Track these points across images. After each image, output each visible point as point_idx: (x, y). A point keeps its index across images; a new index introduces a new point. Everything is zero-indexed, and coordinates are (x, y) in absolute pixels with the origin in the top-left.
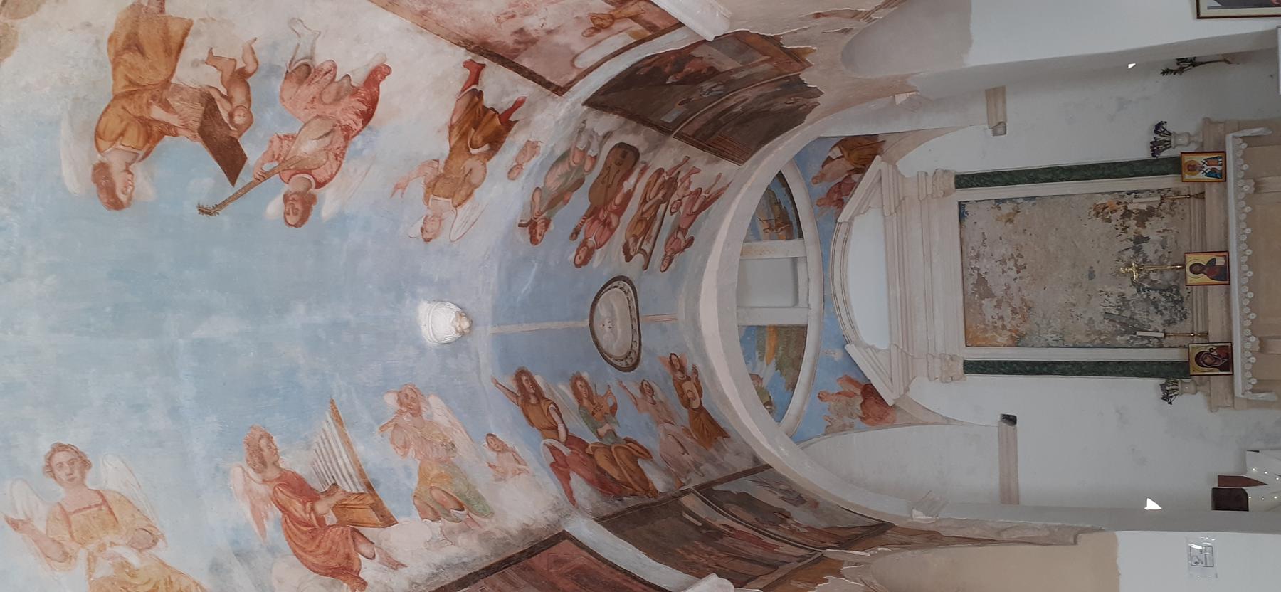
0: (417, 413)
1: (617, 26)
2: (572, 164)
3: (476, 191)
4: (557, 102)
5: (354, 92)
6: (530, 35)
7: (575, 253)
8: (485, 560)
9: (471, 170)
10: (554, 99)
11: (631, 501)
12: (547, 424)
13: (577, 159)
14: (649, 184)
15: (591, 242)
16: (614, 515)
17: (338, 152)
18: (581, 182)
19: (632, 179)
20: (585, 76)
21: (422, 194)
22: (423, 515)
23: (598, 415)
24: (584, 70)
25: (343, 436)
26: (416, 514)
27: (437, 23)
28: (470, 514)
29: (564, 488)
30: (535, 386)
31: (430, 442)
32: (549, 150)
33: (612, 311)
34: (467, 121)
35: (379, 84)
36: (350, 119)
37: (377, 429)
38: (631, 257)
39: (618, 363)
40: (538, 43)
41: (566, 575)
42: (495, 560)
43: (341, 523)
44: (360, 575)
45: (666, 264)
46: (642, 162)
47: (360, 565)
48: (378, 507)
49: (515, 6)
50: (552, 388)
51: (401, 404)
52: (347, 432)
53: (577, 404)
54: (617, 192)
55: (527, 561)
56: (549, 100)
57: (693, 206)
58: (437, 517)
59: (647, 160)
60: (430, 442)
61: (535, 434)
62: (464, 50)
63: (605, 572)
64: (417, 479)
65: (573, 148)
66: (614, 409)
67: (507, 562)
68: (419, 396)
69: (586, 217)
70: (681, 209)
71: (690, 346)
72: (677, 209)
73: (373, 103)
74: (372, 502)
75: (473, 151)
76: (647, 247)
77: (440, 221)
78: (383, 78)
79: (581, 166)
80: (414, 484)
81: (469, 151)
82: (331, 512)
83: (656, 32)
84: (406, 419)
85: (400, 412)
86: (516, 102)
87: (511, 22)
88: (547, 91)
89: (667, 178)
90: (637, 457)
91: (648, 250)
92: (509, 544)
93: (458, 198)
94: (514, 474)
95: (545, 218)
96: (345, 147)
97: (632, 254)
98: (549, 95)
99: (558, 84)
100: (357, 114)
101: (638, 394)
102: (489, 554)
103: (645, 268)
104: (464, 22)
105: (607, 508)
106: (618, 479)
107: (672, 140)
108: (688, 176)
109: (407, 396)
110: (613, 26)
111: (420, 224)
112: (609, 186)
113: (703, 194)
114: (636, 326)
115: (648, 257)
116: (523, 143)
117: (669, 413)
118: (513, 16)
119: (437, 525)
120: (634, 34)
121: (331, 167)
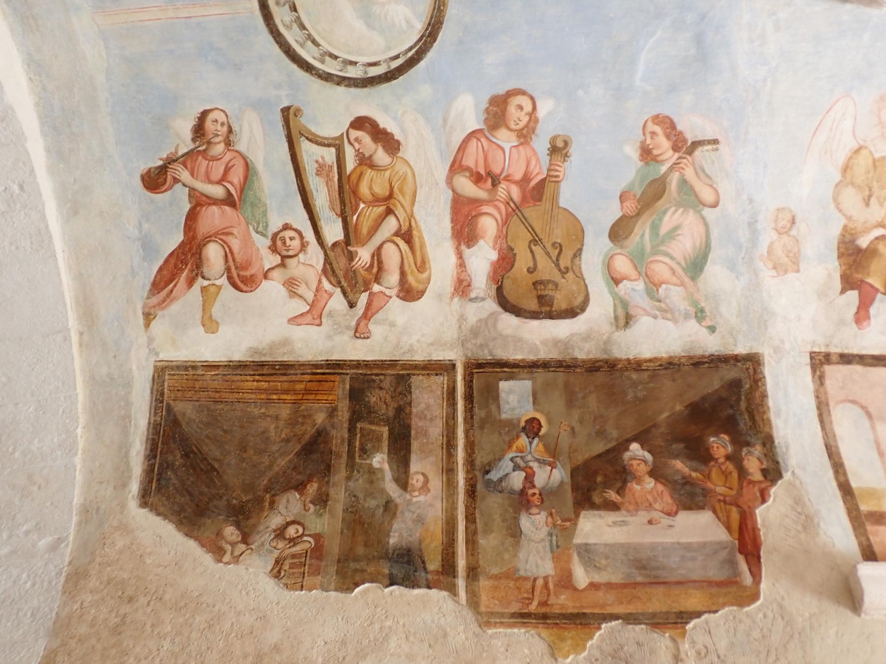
3: (838, 177)
9: (867, 204)
15: (506, 139)
79: (639, 260)
88: (839, 350)
93: (863, 162)
112: (536, 240)
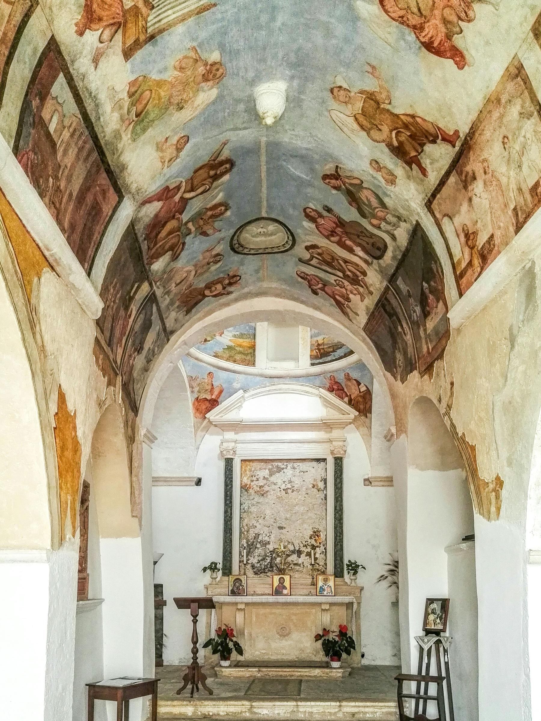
0: (205, 78)
1: (467, 250)
2: (377, 210)
4: (421, 202)
5: (449, 37)
6: (470, 185)
7: (314, 208)
8: (102, 135)
10: (424, 199)
11: (144, 247)
12: (195, 183)
13: (380, 214)
14: (357, 265)
15: (321, 221)
16: (136, 234)
17: (405, 19)
18: (363, 215)
19: (361, 253)
20: (437, 224)
21: (367, 89)
22: (132, 84)
23: (201, 222)
24: (441, 223)
25: (189, 15)
26: (132, 78)
27: (490, 112)
28: (134, 123)
29: (154, 196)
30: (223, 174)
31: (184, 89)
32: (388, 193)
33: (271, 235)
34: (416, 129)
35: (452, 58)
36: (429, 31)
37: (195, 44)
38: (308, 251)
39: (236, 237)
40: (463, 191)
41: (95, 199)
42: (102, 142)
43: (125, 12)
44: (87, 30)
45: (302, 275)
46: (372, 262)
47: (95, 30)
48: (137, 45)
49: (492, 175)
51: (211, 65)
52: (192, 18)
53: (208, 206)
54: (354, 242)
55: (102, 169)
56: (423, 196)
57: (339, 295)
58: (131, 95)
59: (373, 265)
60: (184, 89)
61: (188, 174)
62: (468, 132)
63: (99, 228)
64: (157, 79)
65: (386, 211)
66: (205, 234)
67: (102, 154)
68: (218, 80)
69: (339, 218)
70: (338, 288)
71: (246, 290)
72: (338, 285)
73: (438, 52)
74: (141, 41)
75: (394, 133)
76: (314, 262)
77: (345, 102)
78: (456, 63)
79: (375, 216)
80: (155, 76)
81: (394, 130)
82: (133, 4)
83: (459, 278)
84: (201, 70)
85: (206, 64)
86: (425, 170)
87: (482, 171)
88: (430, 194)
89: (360, 278)
90: (173, 250)
91: (312, 263)
92: (114, 154)
93: (361, 119)
94: (162, 158)
95: (341, 186)
96: (408, 26)
97: (310, 251)
98: (427, 196)
99: (433, 204)
100: (431, 38)
101: (214, 252)
102: (106, 138)
103: (300, 260)
104: (487, 134)
105: (140, 228)
106: (159, 237)
107: (385, 283)
108: (359, 293)
109: (218, 70)
110: (467, 247)
111: (345, 86)
112: (358, 236)
113: (346, 303)
114: (260, 251)
115: (307, 262)
116: (395, 173)
117: (202, 274)
118: (485, 173)
119: (125, 95)
120: (459, 262)
121: (394, 12)
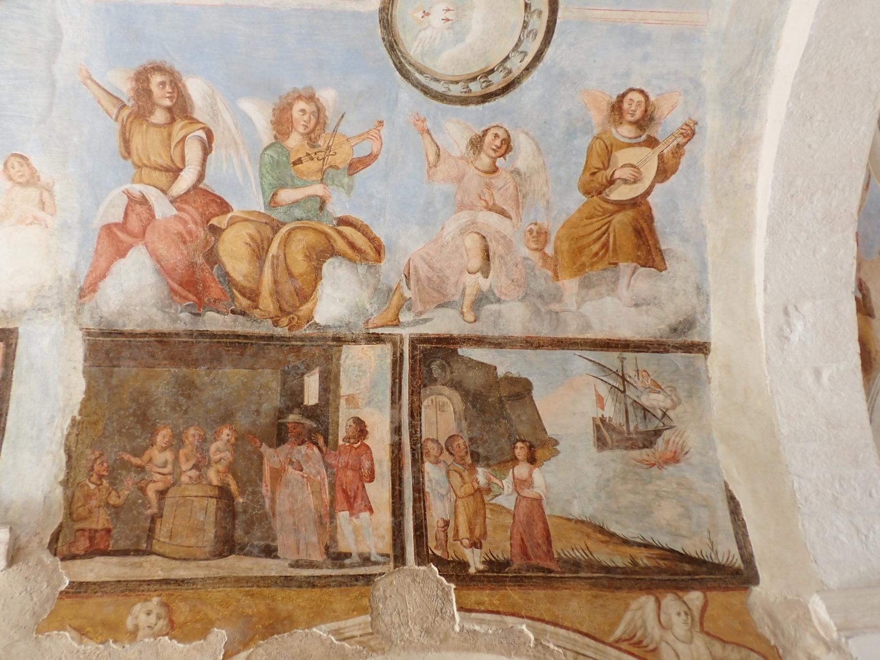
50: (221, 106)
